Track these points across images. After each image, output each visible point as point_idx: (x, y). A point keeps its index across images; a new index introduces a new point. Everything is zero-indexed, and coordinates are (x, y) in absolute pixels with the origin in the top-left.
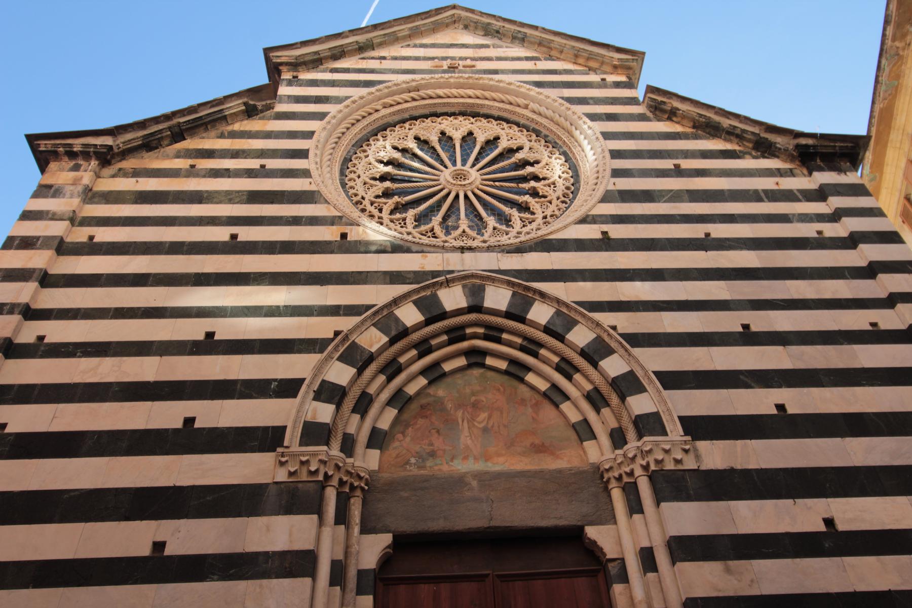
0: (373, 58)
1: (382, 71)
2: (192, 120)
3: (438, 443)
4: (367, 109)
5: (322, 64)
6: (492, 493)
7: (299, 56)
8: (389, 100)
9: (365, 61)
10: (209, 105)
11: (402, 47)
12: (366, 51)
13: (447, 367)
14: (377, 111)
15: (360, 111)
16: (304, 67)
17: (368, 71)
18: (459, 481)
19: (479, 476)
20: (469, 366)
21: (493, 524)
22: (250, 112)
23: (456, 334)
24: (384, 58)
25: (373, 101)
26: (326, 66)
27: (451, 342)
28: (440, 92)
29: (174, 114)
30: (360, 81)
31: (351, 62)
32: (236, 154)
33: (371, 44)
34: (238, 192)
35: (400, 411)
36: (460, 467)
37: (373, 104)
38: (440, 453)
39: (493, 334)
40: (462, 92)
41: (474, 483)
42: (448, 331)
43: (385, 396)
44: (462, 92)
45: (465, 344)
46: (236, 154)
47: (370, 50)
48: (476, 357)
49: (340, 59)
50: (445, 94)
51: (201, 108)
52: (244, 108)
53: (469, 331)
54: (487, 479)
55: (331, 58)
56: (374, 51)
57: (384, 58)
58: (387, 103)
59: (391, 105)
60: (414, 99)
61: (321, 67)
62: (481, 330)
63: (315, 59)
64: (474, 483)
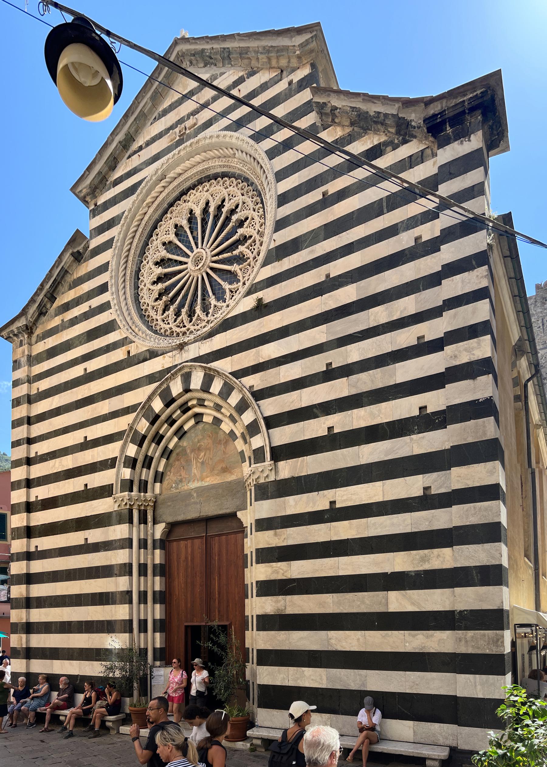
0: (135, 152)
1: (141, 167)
2: (52, 283)
3: (183, 473)
4: (138, 217)
5: (107, 181)
6: (201, 499)
7: (90, 183)
8: (149, 200)
9: (130, 159)
10: (55, 268)
11: (151, 124)
12: (129, 147)
13: (186, 427)
14: (145, 213)
15: (134, 222)
16: (98, 190)
17: (132, 172)
18: (188, 495)
19: (197, 490)
20: (197, 423)
21: (201, 515)
22: (78, 258)
23: (185, 408)
24: (141, 148)
25: (138, 208)
26: (110, 181)
27: (184, 412)
28: (178, 170)
29: (42, 285)
30: (128, 189)
31: (121, 170)
32: (78, 301)
33: (130, 136)
34: (83, 333)
35: (167, 459)
36: (191, 486)
37: (140, 210)
38: (184, 479)
39: (201, 403)
40: (193, 160)
41: (195, 495)
42: (180, 407)
43: (158, 454)
44: (193, 160)
45: (190, 413)
46: (78, 301)
47: (132, 143)
48: (198, 417)
49: (116, 167)
50: (183, 170)
51: (53, 272)
52: (72, 258)
53: (190, 404)
54: (201, 491)
55: (110, 170)
56: (135, 142)
57: (141, 148)
58: (149, 203)
59: (153, 202)
60: (164, 187)
61: (108, 183)
62: (194, 402)
63: (100, 180)
64: (195, 495)
